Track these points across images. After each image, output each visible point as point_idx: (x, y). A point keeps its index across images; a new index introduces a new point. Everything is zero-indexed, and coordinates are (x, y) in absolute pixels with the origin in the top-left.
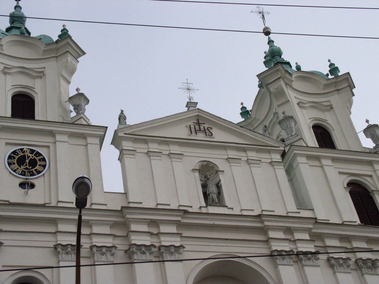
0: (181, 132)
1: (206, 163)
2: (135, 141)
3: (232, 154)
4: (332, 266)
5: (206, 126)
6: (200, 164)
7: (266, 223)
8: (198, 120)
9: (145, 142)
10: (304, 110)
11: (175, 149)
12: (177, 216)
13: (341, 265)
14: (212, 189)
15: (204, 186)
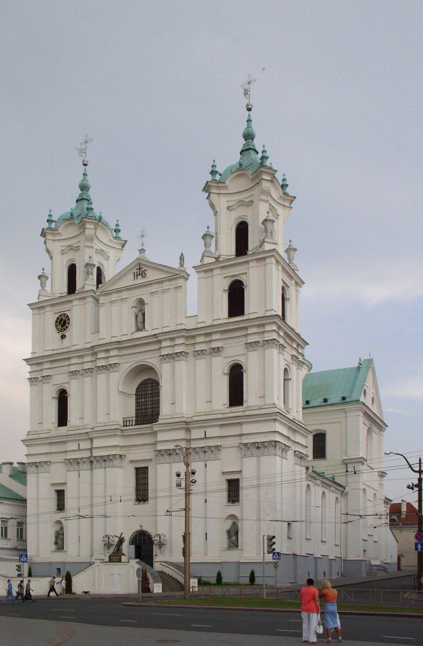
0: (129, 281)
1: (139, 300)
2: (105, 295)
3: (154, 288)
4: (195, 356)
5: (143, 270)
6: (137, 301)
7: (159, 338)
8: (140, 265)
9: (110, 294)
10: (232, 212)
11: (125, 294)
12: (116, 345)
13: (199, 354)
14: (140, 319)
15: (137, 317)
